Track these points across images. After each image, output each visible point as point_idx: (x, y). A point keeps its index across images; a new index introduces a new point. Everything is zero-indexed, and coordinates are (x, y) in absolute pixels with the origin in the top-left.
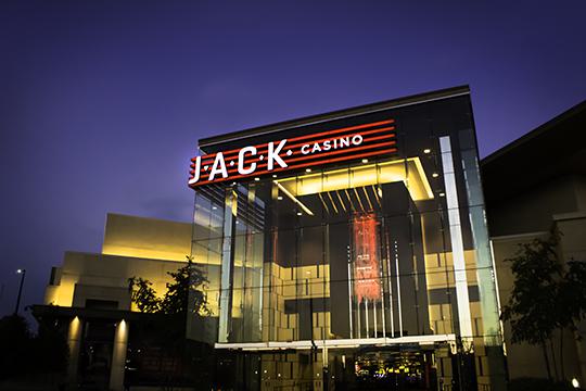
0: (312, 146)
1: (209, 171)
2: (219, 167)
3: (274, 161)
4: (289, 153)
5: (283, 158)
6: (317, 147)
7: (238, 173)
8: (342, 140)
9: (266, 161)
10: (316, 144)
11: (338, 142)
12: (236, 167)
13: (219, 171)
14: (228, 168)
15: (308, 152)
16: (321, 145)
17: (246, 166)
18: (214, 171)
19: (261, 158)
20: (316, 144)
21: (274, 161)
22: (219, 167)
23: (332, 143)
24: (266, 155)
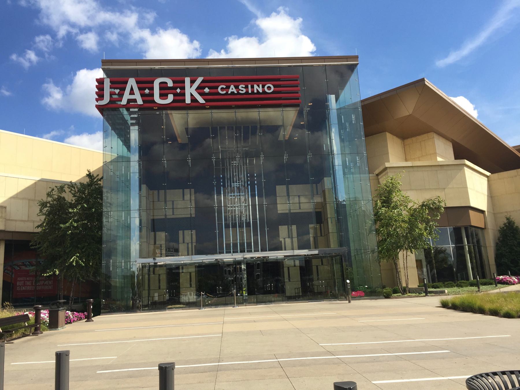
0: (228, 87)
1: (121, 95)
2: (132, 92)
3: (192, 95)
4: (207, 90)
5: (202, 94)
6: (232, 89)
7: (154, 102)
8: (256, 86)
9: (184, 95)
10: (232, 86)
11: (252, 87)
12: (152, 95)
13: (132, 97)
14: (143, 95)
15: (225, 92)
16: (237, 87)
17: (163, 96)
18: (127, 96)
19: (178, 90)
20: (232, 86)
21: (192, 95)
22: (132, 92)
23: (247, 87)
24: (183, 88)
